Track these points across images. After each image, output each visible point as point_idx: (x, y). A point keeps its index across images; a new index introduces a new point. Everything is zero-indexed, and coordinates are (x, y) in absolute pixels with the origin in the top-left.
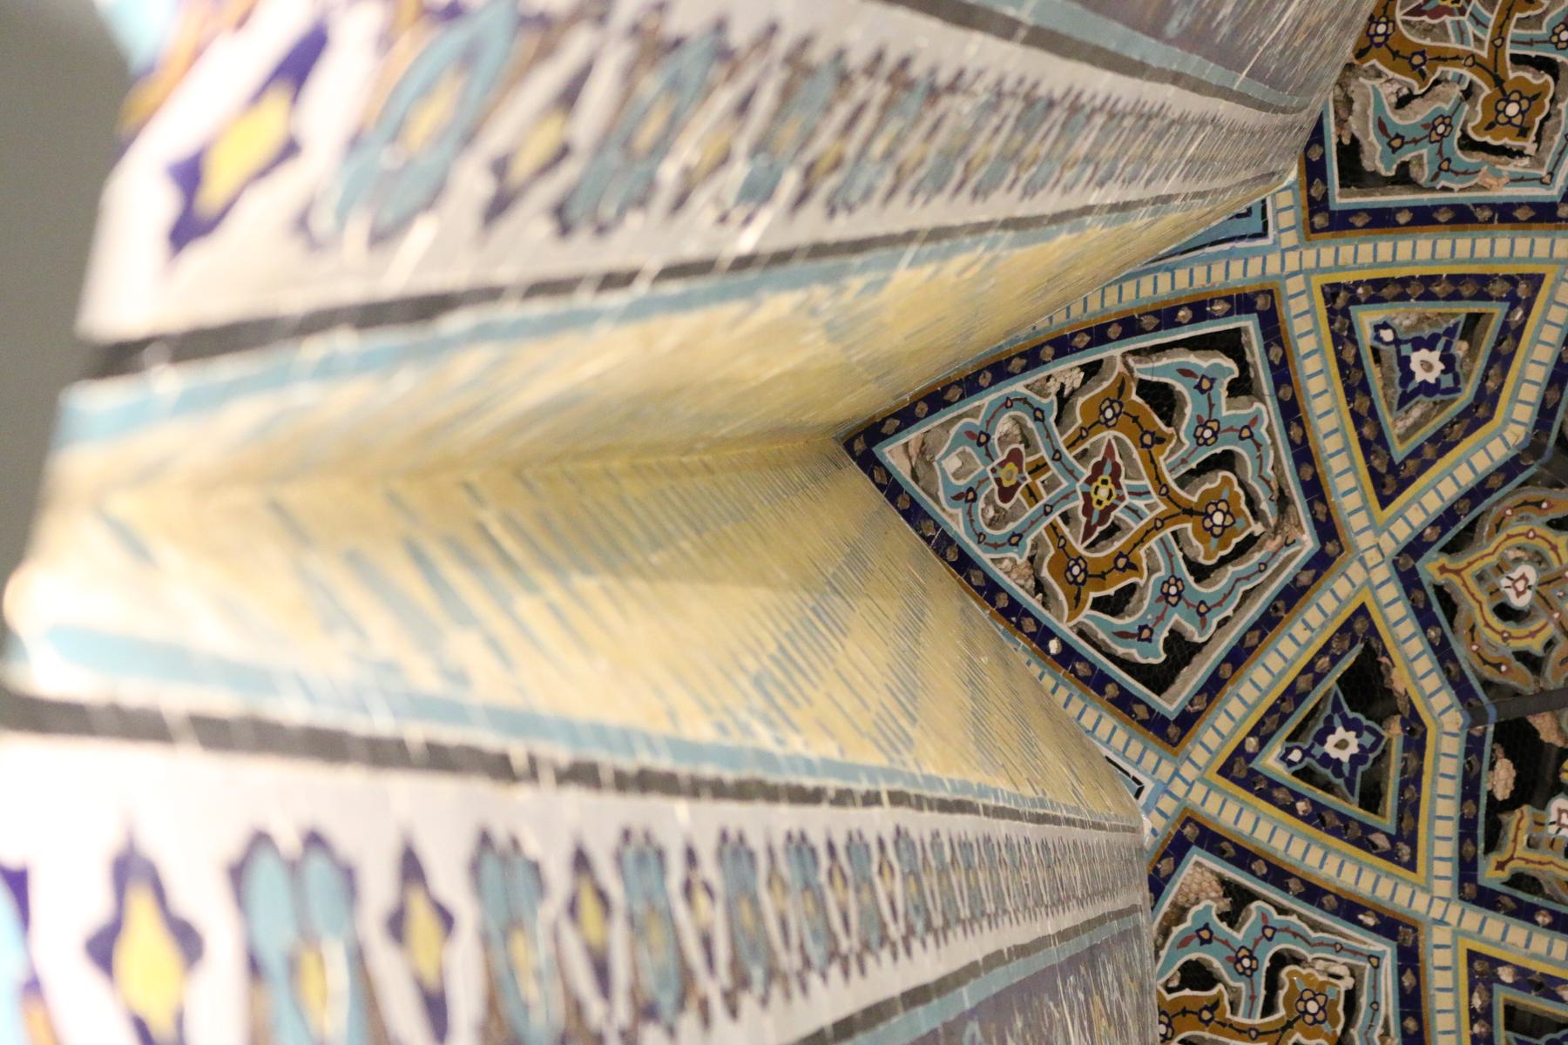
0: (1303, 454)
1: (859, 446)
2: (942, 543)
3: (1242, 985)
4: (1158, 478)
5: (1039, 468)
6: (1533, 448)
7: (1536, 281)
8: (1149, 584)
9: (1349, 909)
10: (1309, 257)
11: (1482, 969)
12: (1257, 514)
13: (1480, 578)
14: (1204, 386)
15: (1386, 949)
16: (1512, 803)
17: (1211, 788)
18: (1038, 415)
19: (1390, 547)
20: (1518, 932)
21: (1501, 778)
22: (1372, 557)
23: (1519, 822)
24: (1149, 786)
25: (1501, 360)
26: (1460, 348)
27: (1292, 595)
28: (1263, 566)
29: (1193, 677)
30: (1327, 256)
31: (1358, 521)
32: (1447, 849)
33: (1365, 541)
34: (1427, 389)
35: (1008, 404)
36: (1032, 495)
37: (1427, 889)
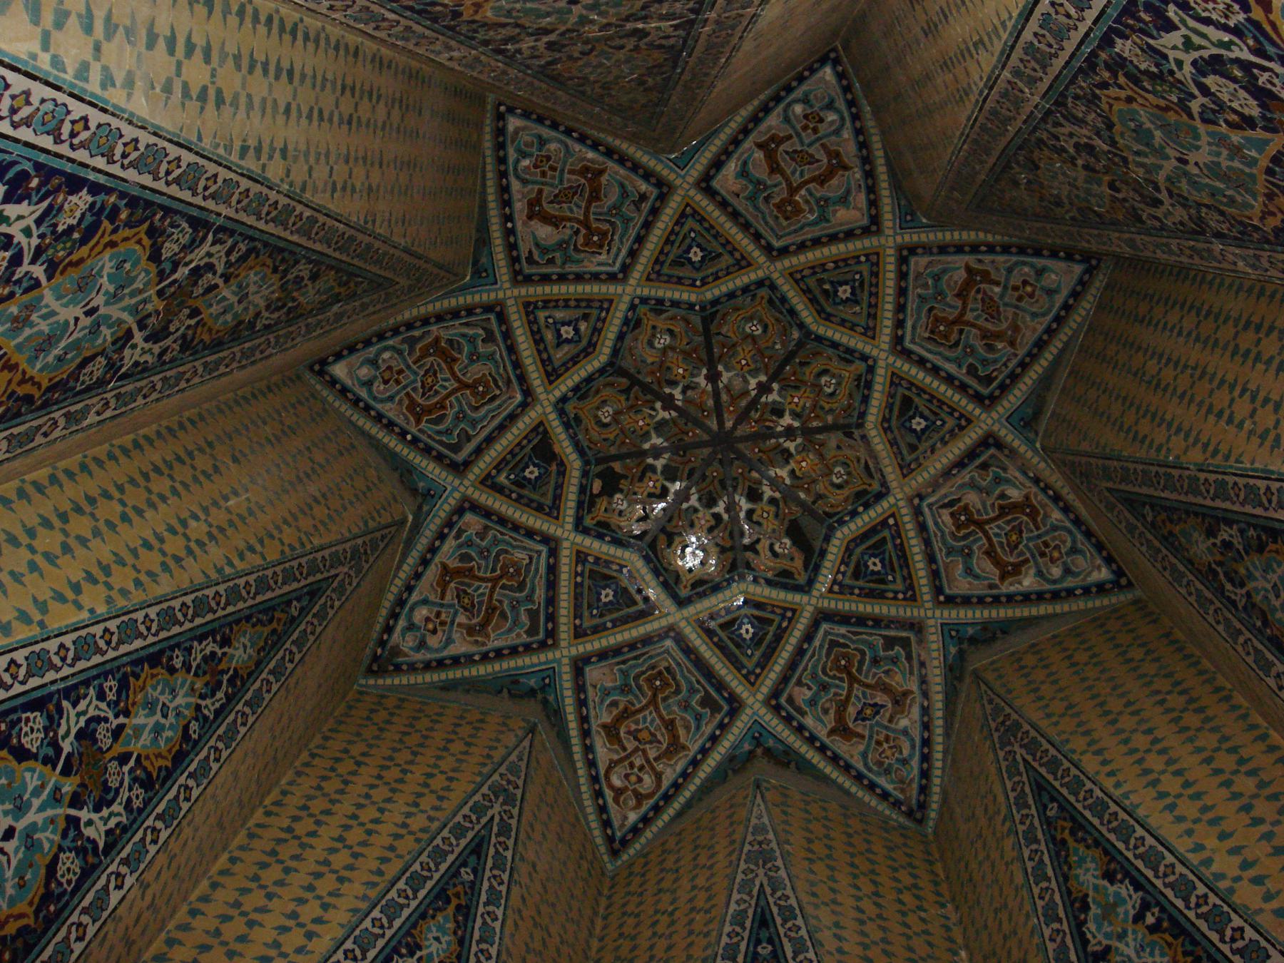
0: (517, 365)
1: (317, 367)
3: (483, 563)
4: (453, 374)
5: (400, 372)
6: (611, 364)
8: (451, 413)
9: (530, 533)
10: (516, 292)
11: (581, 557)
12: (498, 387)
14: (472, 340)
15: (544, 549)
16: (600, 495)
18: (400, 352)
19: (552, 399)
21: (597, 486)
22: (546, 403)
23: (602, 504)
26: (583, 326)
27: (512, 417)
28: (500, 406)
29: (469, 448)
30: (523, 291)
31: (540, 390)
32: (571, 512)
33: (543, 397)
34: (568, 341)
35: (386, 349)
36: (398, 382)
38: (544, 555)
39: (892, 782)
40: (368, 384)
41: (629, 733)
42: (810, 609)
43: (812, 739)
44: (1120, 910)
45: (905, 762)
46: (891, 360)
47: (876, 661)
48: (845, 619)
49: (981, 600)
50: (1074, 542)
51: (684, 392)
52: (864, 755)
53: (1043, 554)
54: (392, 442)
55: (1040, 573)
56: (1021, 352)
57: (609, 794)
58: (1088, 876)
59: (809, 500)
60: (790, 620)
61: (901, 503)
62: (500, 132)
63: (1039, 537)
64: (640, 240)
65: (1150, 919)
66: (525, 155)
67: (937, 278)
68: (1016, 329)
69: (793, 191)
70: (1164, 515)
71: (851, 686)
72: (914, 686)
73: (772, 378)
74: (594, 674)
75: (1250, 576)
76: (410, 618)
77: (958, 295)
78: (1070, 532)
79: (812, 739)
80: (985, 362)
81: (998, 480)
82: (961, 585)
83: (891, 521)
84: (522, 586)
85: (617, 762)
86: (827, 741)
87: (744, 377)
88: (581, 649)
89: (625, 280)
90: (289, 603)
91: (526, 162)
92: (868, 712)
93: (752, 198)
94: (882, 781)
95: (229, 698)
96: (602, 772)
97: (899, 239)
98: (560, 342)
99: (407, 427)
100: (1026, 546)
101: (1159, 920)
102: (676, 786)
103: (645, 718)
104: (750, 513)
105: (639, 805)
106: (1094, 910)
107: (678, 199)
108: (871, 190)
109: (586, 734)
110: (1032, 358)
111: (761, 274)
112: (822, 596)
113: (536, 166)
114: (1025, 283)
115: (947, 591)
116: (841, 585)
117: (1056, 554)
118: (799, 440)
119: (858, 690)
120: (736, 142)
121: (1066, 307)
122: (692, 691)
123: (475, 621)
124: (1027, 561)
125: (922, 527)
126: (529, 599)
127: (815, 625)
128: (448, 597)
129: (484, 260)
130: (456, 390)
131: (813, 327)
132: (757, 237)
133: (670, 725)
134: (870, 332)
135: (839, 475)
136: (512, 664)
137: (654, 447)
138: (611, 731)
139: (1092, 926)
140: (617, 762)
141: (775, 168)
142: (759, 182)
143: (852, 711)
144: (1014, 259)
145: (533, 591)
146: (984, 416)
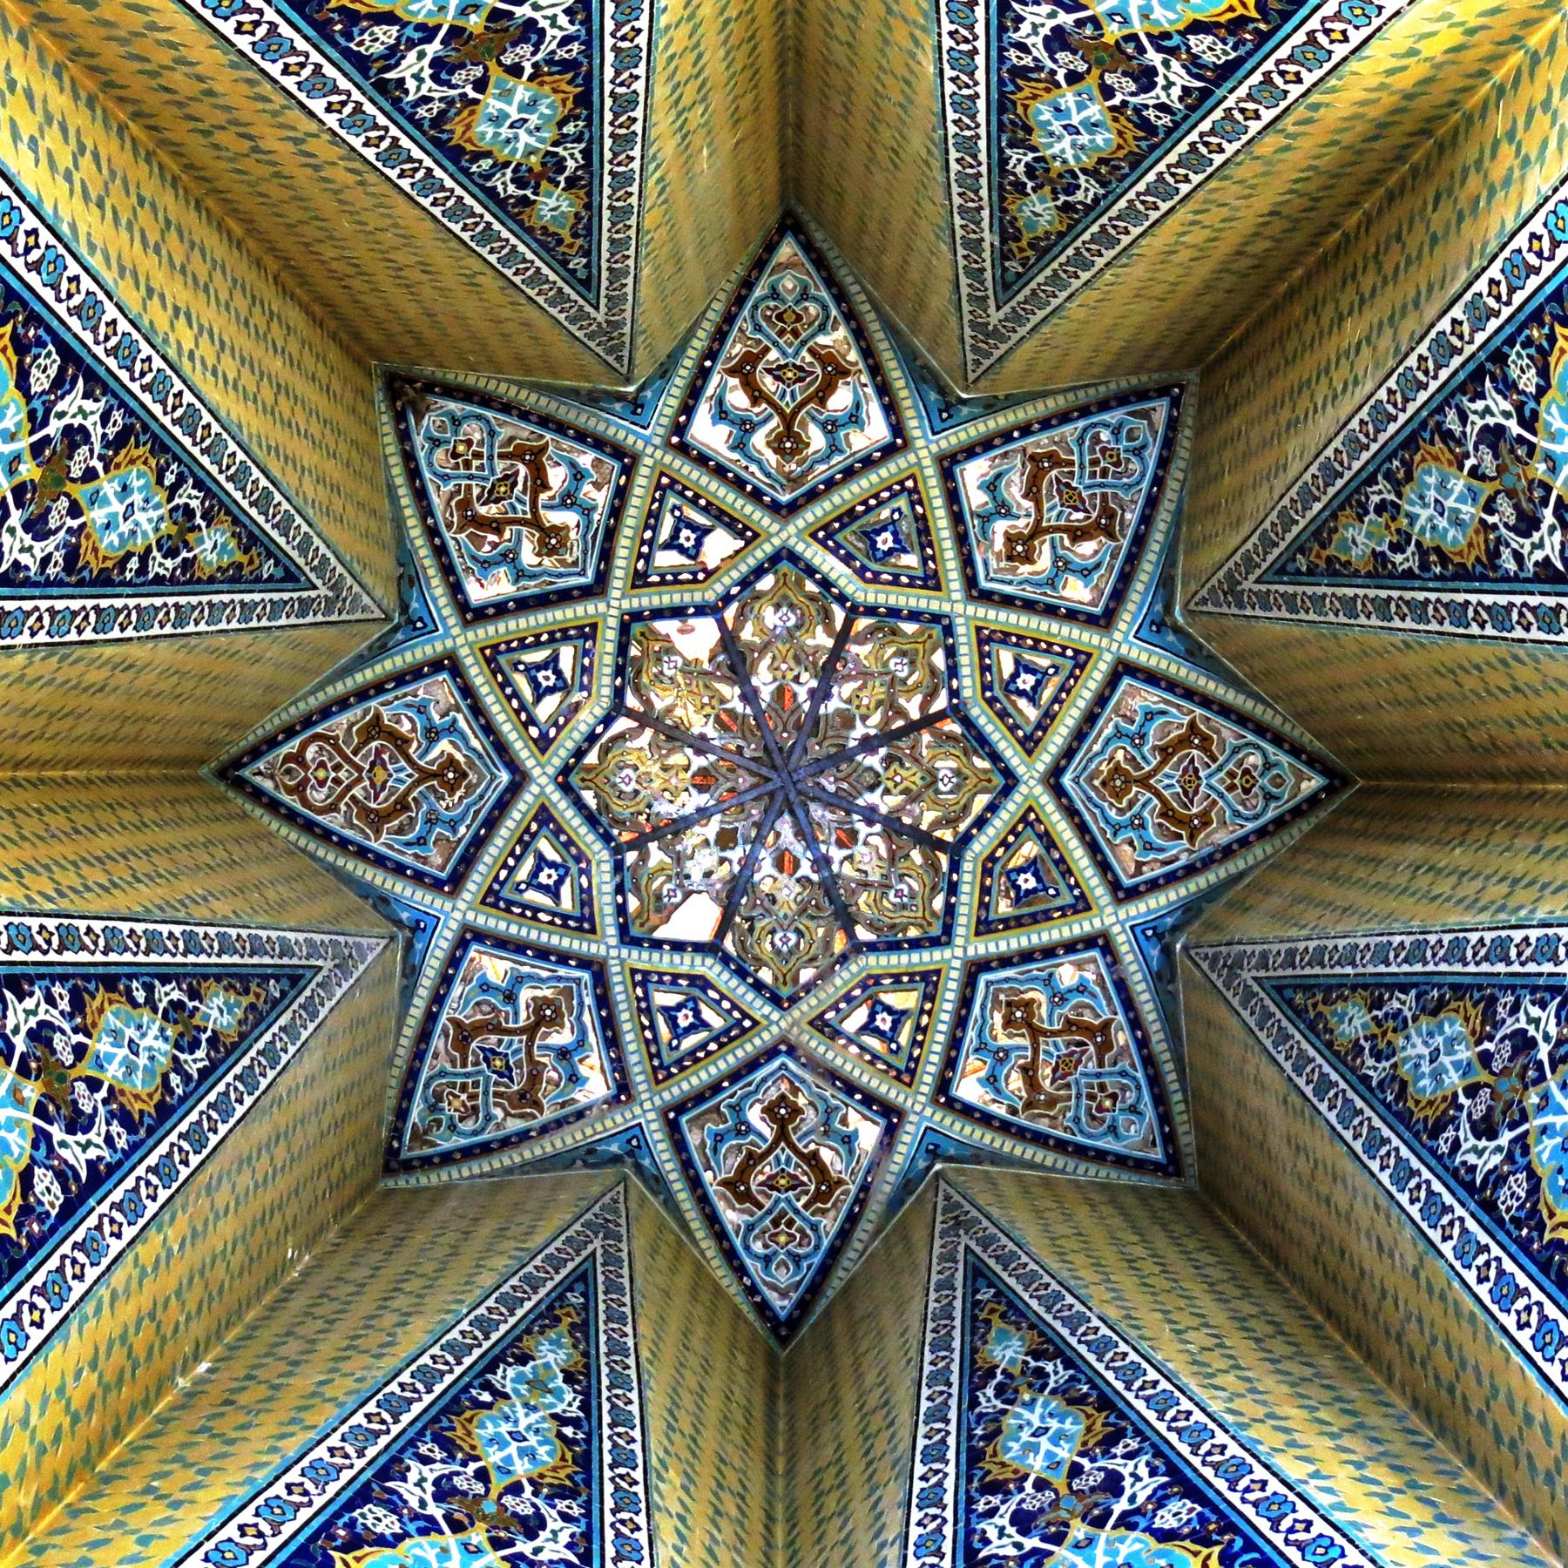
0: (831, 484)
2: (748, 284)
5: (795, 334)
7: (938, 588)
9: (607, 555)
10: (927, 462)
11: (587, 632)
13: (785, 597)
17: (652, 468)
19: (792, 542)
22: (784, 535)
24: (647, 432)
27: (756, 495)
30: (930, 472)
31: (800, 523)
33: (791, 529)
35: (825, 307)
36: (781, 333)
37: (623, 596)
38: (582, 580)
39: (422, 1120)
40: (774, 294)
41: (378, 752)
42: (603, 951)
43: (438, 999)
44: (549, 1399)
45: (452, 1127)
46: (957, 964)
47: (563, 1054)
50: (807, 1256)
51: (838, 712)
52: (442, 1073)
53: (776, 1223)
54: (699, 343)
55: (750, 1228)
56: (1021, 1120)
57: (293, 746)
60: (580, 929)
61: (774, 1029)
62: (1142, 395)
63: (797, 1212)
64: (1029, 606)
66: (1116, 432)
68: (1052, 1102)
69: (1144, 782)
70: (1002, 1308)
71: (522, 1031)
72: (548, 1115)
75: (1030, 1405)
77: (1069, 1022)
78: (817, 1247)
79: (438, 999)
82: (693, 1139)
83: (747, 1023)
85: (336, 747)
86: (443, 1019)
87: (878, 784)
88: (469, 661)
89: (970, 598)
90: (587, 254)
91: (1105, 435)
93: (1119, 734)
95: (501, 203)
96: (319, 729)
97: (1116, 929)
99: (722, 358)
100: (777, 1201)
101: (575, 1442)
102: (326, 835)
103: (401, 770)
105: (290, 791)
106: (527, 1369)
107: (1095, 640)
108: (1171, 879)
109: (362, 695)
111: (1021, 770)
112: (622, 962)
113: (1103, 451)
114: (1114, 1097)
115: (684, 1119)
116: (644, 984)
117: (782, 1239)
118: (815, 877)
119: (519, 1041)
120: (1189, 694)
121: (1101, 1156)
123: (483, 510)
124: (760, 1206)
125: (753, 1065)
127: (585, 963)
128: (500, 466)
129: (965, 410)
130: (780, 412)
131: (969, 855)
132: (1069, 753)
133: (402, 805)
134: (984, 927)
135: (785, 940)
136: (431, 572)
138: (375, 727)
139: (511, 1372)
140: (336, 747)
141: (1165, 752)
142: (1143, 737)
143: (494, 1038)
144: (1140, 1075)
145: (533, 576)
146: (922, 1099)
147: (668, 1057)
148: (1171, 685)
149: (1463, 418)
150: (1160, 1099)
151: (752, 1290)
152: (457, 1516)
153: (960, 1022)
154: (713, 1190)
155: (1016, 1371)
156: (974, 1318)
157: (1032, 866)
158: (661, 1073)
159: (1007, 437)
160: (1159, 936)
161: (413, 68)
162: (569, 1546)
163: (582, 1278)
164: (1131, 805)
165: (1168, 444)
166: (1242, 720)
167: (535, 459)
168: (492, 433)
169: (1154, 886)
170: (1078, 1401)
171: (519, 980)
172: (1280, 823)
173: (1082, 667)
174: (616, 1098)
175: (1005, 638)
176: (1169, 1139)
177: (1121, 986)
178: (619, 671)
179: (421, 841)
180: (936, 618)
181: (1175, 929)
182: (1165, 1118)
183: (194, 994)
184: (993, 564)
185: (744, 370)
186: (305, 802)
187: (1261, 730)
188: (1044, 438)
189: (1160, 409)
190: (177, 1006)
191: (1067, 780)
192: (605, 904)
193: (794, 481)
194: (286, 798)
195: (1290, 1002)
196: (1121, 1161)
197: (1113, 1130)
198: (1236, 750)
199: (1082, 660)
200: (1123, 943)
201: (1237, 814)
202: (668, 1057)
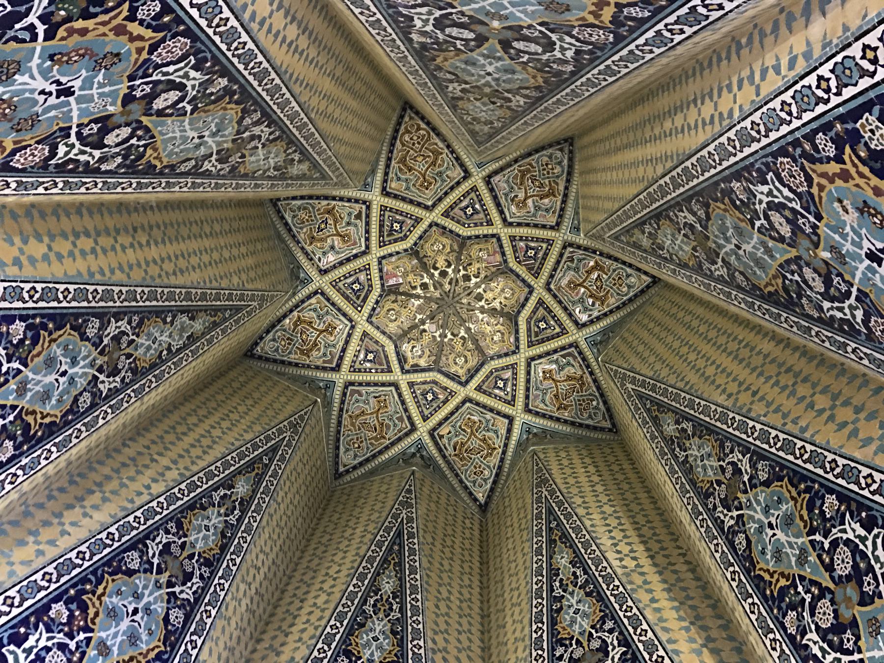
0: (560, 302)
9: (519, 225)
11: (490, 223)
15: (510, 220)
20: (485, 232)
25: (529, 330)
27: (552, 276)
40: (628, 276)
43: (341, 199)
45: (294, 217)
47: (332, 248)
48: (356, 256)
49: (303, 301)
51: (477, 317)
52: (313, 208)
55: (285, 330)
56: (345, 416)
57: (423, 126)
58: (198, 326)
59: (399, 298)
64: (528, 381)
65: (165, 352)
66: (596, 408)
67: (395, 425)
68: (353, 424)
72: (309, 248)
73: (442, 341)
74: (457, 173)
76: (562, 167)
79: (341, 199)
80: (357, 401)
81: (325, 355)
82: (313, 300)
84: (512, 200)
86: (334, 203)
92: (323, 226)
93: (488, 421)
94: (299, 203)
98: (543, 319)
102: (393, 145)
104: (422, 276)
108: (440, 450)
110: (340, 416)
111: (468, 387)
120: (506, 445)
121: (338, 448)
122: (407, 188)
125: (345, 315)
126: (506, 195)
127: (367, 247)
128: (547, 181)
132: (478, 404)
134: (411, 385)
137: (480, 287)
138: (436, 153)
147: (340, 284)
148: (508, 438)
149: (611, 631)
150: (361, 464)
151: (261, 338)
152: (107, 349)
153: (376, 384)
154: (295, 313)
155: (234, 498)
156: (254, 463)
157: (436, 397)
158: (334, 284)
159: (588, 366)
160: (419, 450)
161: (691, 219)
162: (109, 389)
163: (238, 309)
164: (464, 430)
165: (595, 428)
166: (500, 467)
167: (552, 193)
168: (558, 177)
169: (436, 444)
170: (223, 535)
171: (356, 226)
172: (466, 488)
173: (509, 403)
174: (320, 271)
175: (515, 374)
176: (347, 472)
177: (400, 439)
178: (477, 237)
179: (399, 179)
180: (518, 347)
181: (422, 457)
182: (355, 468)
183: (300, 161)
184: (541, 367)
185: (597, 267)
186: (403, 134)
187: (497, 475)
188: (590, 380)
189: (607, 424)
190: (293, 160)
191: (468, 404)
192: (391, 249)
193: (559, 289)
194: (403, 127)
195: (394, 543)
196: (337, 456)
197: (347, 450)
198: (489, 467)
199: (512, 402)
200: (415, 436)
201: (466, 471)
202: (340, 284)
